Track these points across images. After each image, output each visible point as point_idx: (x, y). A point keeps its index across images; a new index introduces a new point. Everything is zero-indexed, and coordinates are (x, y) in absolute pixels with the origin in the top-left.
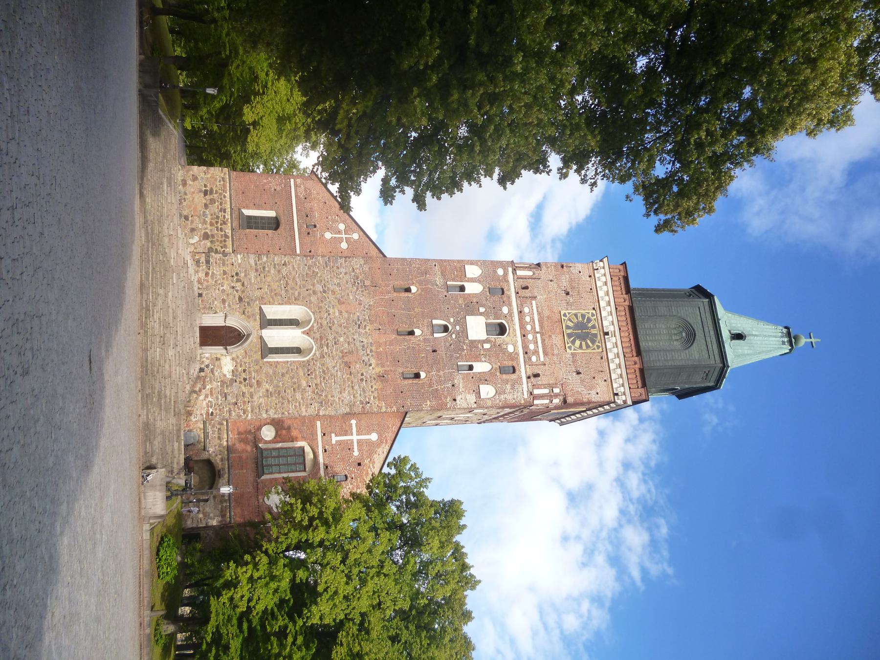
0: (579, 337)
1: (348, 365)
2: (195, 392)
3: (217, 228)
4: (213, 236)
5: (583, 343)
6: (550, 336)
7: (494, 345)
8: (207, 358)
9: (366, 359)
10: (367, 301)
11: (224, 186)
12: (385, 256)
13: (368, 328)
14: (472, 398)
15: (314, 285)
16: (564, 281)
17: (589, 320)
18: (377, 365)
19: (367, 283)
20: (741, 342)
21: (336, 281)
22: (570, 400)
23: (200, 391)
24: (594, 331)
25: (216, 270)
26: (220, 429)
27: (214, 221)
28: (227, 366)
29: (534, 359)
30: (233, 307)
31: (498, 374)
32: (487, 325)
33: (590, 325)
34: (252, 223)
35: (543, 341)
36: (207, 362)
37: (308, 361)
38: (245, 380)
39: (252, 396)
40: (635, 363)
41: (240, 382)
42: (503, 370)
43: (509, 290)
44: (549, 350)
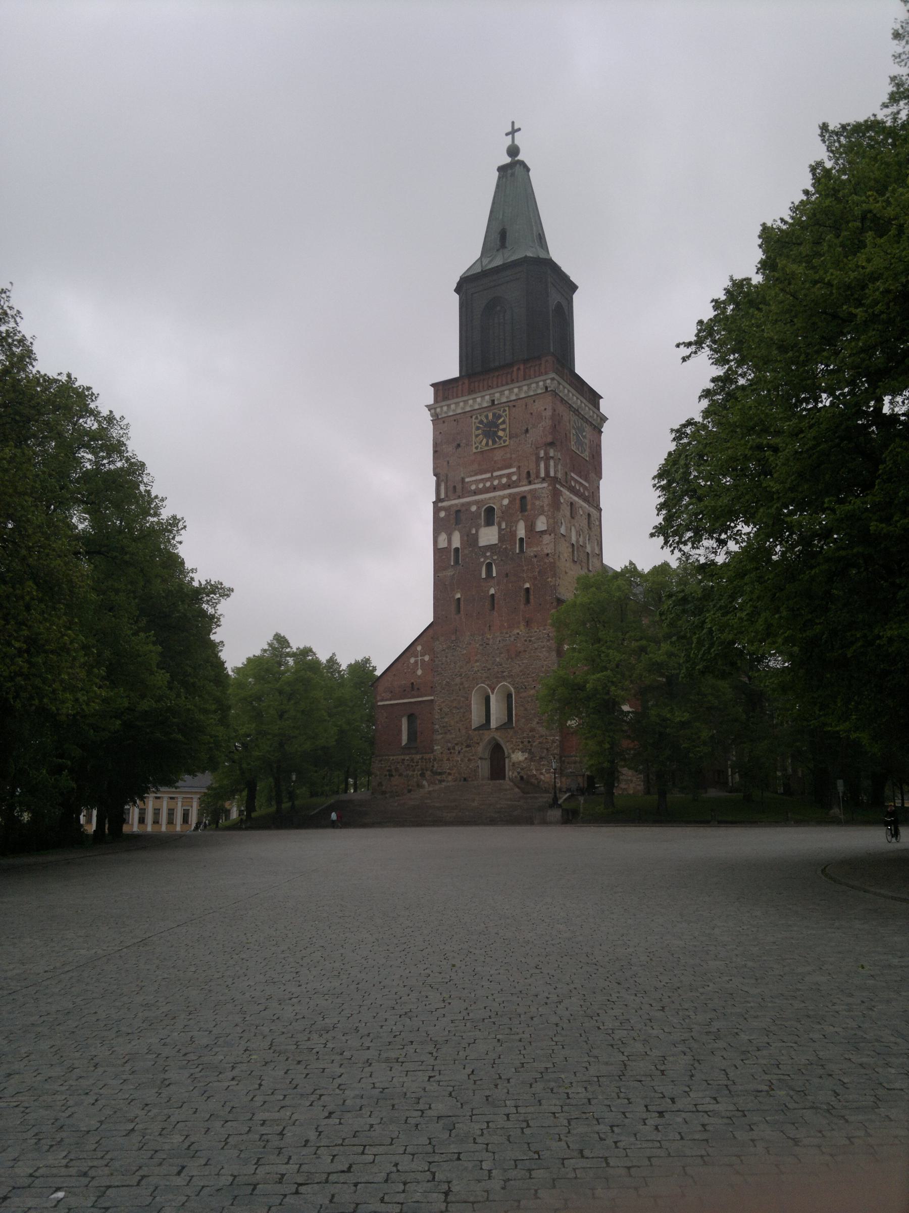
0: (496, 433)
1: (518, 654)
4: (422, 769)
5: (501, 427)
6: (495, 462)
7: (502, 518)
9: (512, 639)
14: (547, 538)
17: (481, 422)
18: (518, 627)
19: (453, 638)
22: (549, 439)
24: (490, 416)
28: (519, 757)
29: (514, 478)
33: (485, 421)
36: (516, 774)
37: (515, 688)
38: (529, 742)
39: (542, 736)
42: (523, 508)
43: (456, 505)
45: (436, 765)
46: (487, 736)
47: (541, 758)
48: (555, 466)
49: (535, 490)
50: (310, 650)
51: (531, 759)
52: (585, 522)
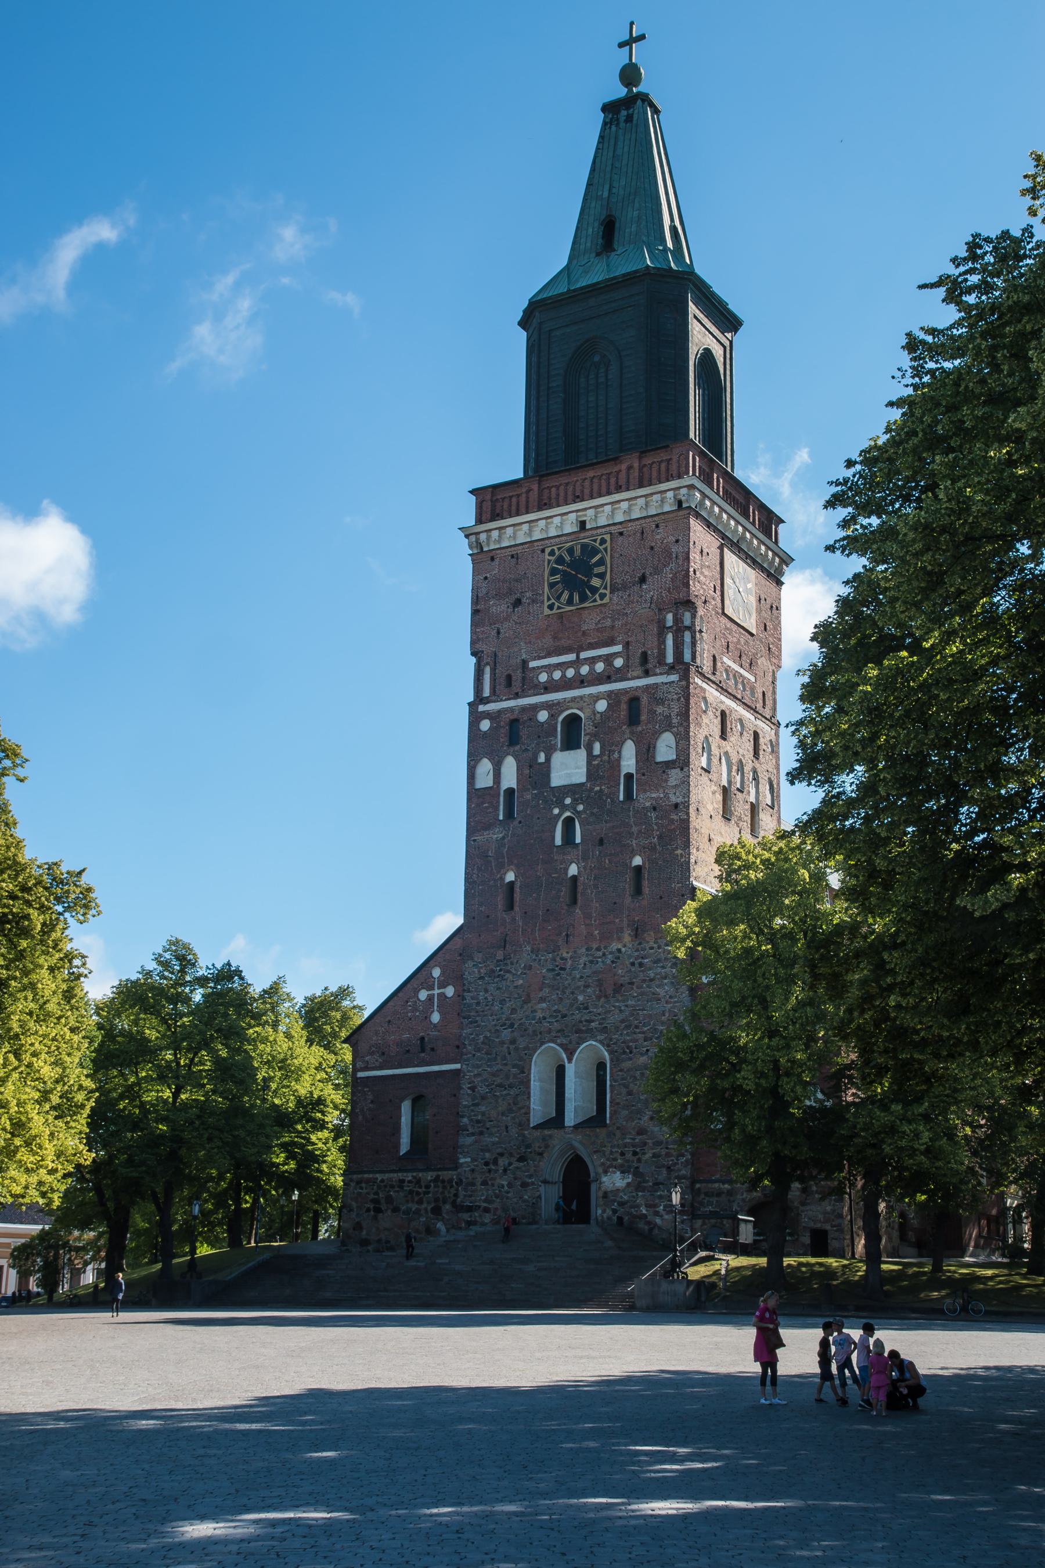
1: (618, 988)
2: (651, 1230)
3: (425, 1193)
4: (436, 1200)
5: (596, 570)
8: (604, 1211)
10: (525, 956)
11: (368, 1181)
13: (565, 955)
14: (674, 775)
15: (503, 1043)
16: (499, 608)
18: (619, 939)
19: (500, 955)
20: (617, 225)
23: (649, 1223)
24: (578, 551)
26: (706, 1194)
27: (416, 1198)
28: (615, 1181)
29: (619, 662)
30: (532, 1170)
31: (640, 728)
33: (567, 558)
36: (609, 1212)
37: (610, 1052)
38: (635, 1153)
39: (658, 1143)
41: (639, 1160)
42: (634, 718)
43: (511, 710)
45: (462, 1193)
46: (558, 1139)
49: (656, 686)
50: (238, 973)
51: (639, 1187)
52: (750, 746)
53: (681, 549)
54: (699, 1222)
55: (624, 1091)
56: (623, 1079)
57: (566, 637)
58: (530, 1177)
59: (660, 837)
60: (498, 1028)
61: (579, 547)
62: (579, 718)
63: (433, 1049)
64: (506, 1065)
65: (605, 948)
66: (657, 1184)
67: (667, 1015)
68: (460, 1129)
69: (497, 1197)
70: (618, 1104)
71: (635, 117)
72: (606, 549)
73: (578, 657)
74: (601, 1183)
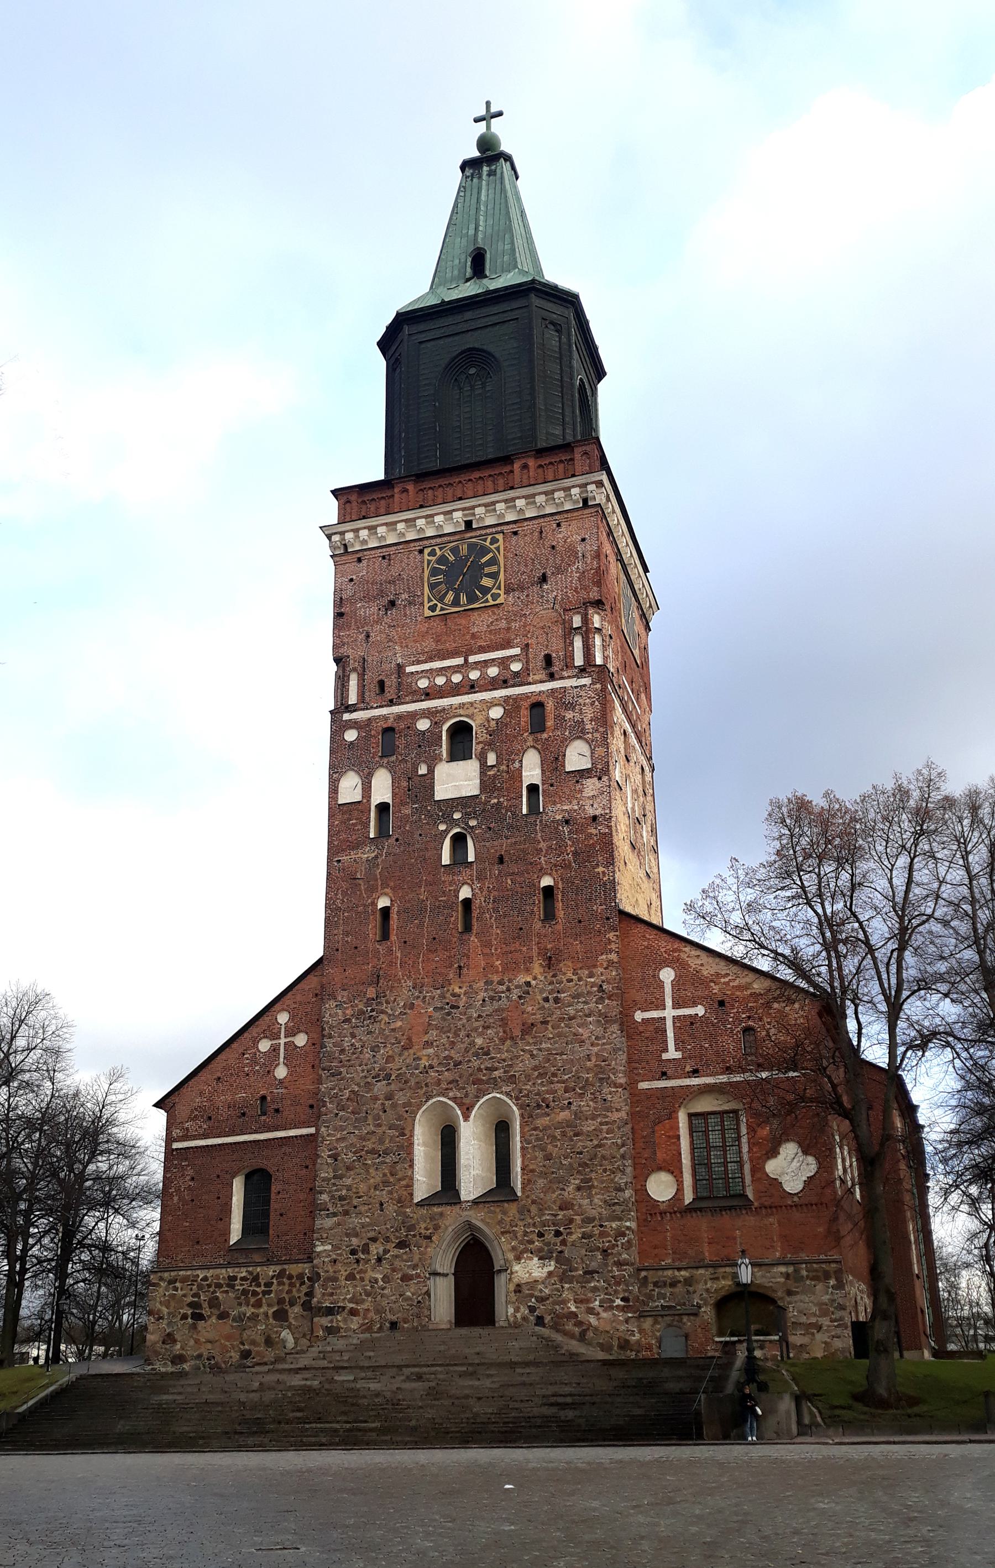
1: (528, 1029)
2: (583, 1334)
3: (264, 1293)
4: (281, 1301)
5: (487, 570)
6: (474, 636)
8: (517, 1310)
10: (405, 992)
11: (184, 1280)
12: (320, 961)
13: (457, 990)
14: (591, 786)
15: (376, 1098)
16: (369, 610)
18: (528, 970)
19: (371, 992)
21: (368, 1054)
23: (579, 1324)
24: (464, 550)
25: (345, 1294)
26: (656, 1284)
27: (252, 1300)
28: (532, 1270)
29: (516, 667)
30: (416, 1258)
31: (545, 736)
32: (453, 758)
33: (452, 558)
34: (256, 1221)
35: (482, 650)
36: (524, 1311)
37: (521, 1107)
38: (558, 1234)
39: (589, 1220)
40: (525, 467)
41: (564, 1243)
42: (538, 725)
43: (385, 718)
44: (499, 638)
46: (452, 1219)
47: (589, 1273)
48: (604, 648)
53: (588, 547)
54: (649, 1321)
55: (540, 1155)
56: (538, 1139)
57: (450, 640)
58: (415, 1267)
59: (575, 854)
60: (369, 1080)
61: (465, 546)
62: (470, 728)
63: (277, 1111)
64: (379, 1125)
65: (510, 981)
66: (589, 1273)
67: (594, 1059)
68: (313, 1210)
69: (368, 1294)
70: (533, 1171)
71: (498, 172)
72: (498, 549)
73: (466, 660)
74: (512, 1273)
